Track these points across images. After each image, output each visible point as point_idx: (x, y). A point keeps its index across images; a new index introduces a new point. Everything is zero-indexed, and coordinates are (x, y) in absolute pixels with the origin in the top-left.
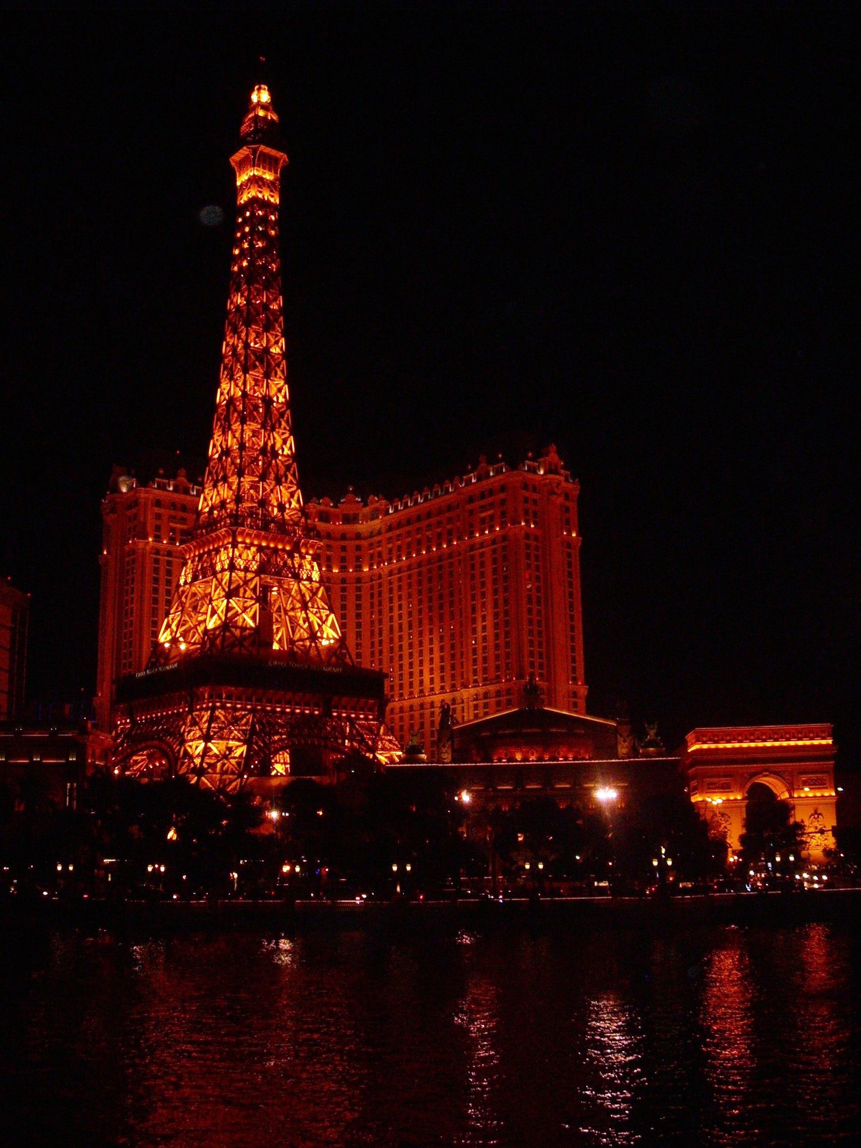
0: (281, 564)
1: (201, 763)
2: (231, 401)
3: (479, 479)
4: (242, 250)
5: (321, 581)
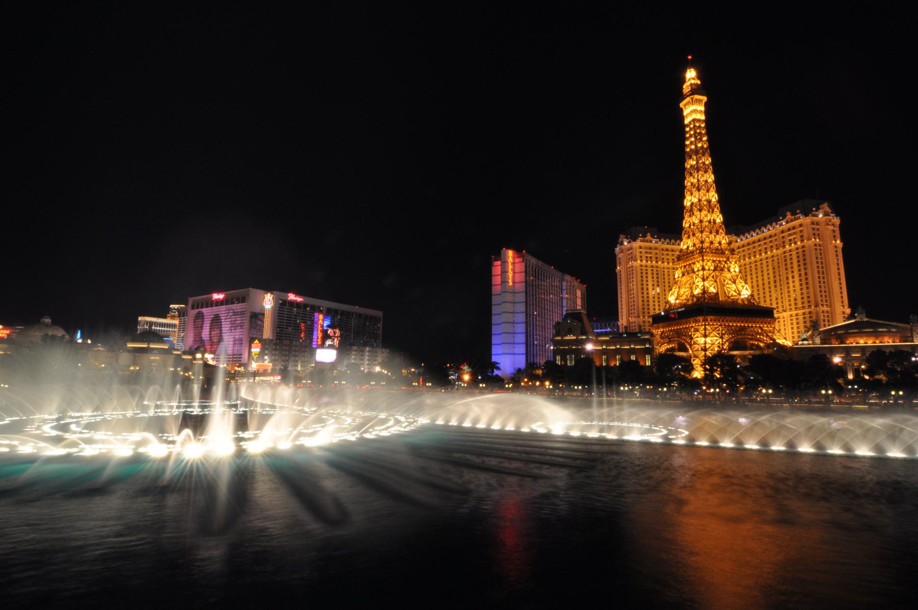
2: (692, 204)
3: (787, 222)
4: (691, 143)
5: (740, 272)
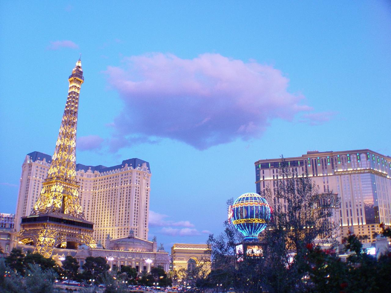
0: (69, 191)
1: (43, 243)
